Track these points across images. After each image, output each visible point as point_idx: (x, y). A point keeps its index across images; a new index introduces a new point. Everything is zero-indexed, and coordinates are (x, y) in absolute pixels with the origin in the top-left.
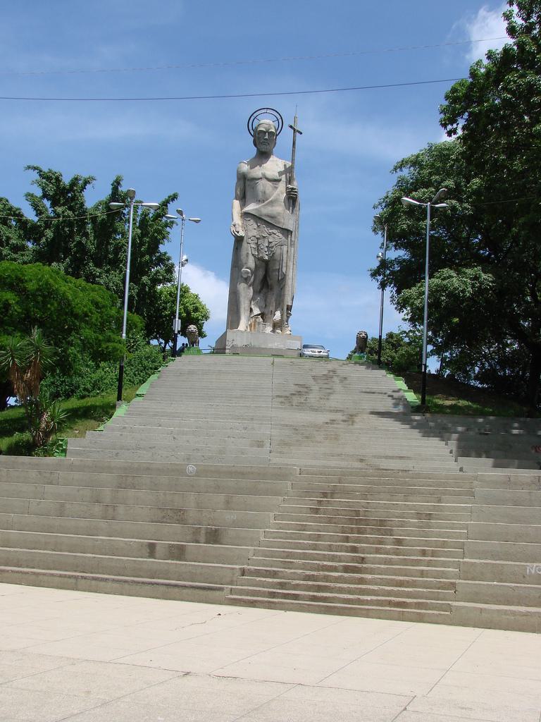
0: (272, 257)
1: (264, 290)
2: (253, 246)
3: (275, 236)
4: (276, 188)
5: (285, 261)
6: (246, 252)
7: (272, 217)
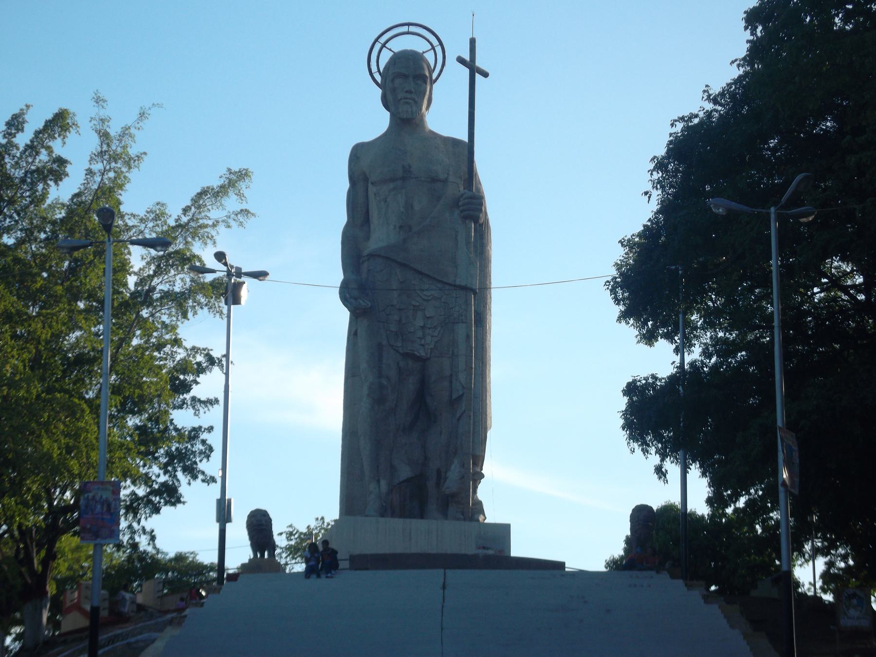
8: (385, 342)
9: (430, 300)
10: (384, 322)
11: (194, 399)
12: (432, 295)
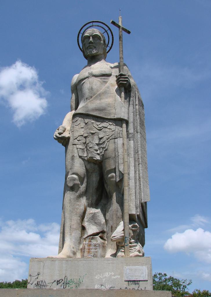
0: (104, 158)
1: (103, 201)
3: (107, 130)
4: (106, 82)
5: (121, 156)
6: (71, 155)
9: (101, 130)
10: (76, 145)
12: (103, 126)
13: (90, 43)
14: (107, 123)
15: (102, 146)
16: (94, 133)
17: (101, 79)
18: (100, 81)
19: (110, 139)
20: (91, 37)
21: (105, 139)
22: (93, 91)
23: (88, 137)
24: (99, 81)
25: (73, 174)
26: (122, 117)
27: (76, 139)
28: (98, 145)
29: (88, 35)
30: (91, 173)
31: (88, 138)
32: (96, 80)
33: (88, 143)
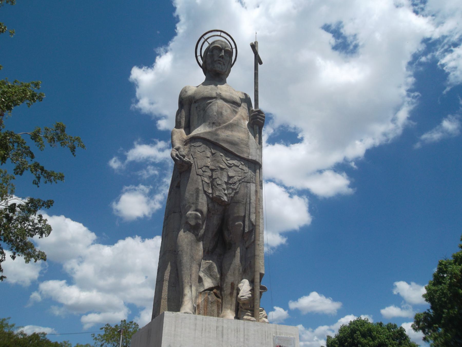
0: (234, 201)
2: (206, 180)
3: (237, 169)
4: (236, 112)
5: (253, 205)
7: (233, 143)
8: (201, 188)
10: (201, 176)
11: (36, 166)
12: (233, 164)
13: (220, 57)
14: (238, 161)
15: (231, 186)
16: (224, 169)
17: (231, 106)
18: (230, 108)
19: (243, 182)
20: (223, 51)
21: (236, 179)
22: (222, 117)
23: (215, 171)
24: (229, 107)
25: (197, 210)
26: (257, 160)
27: (201, 168)
28: (226, 183)
29: (219, 46)
30: (213, 214)
31: (215, 172)
32: (226, 105)
33: (216, 178)
